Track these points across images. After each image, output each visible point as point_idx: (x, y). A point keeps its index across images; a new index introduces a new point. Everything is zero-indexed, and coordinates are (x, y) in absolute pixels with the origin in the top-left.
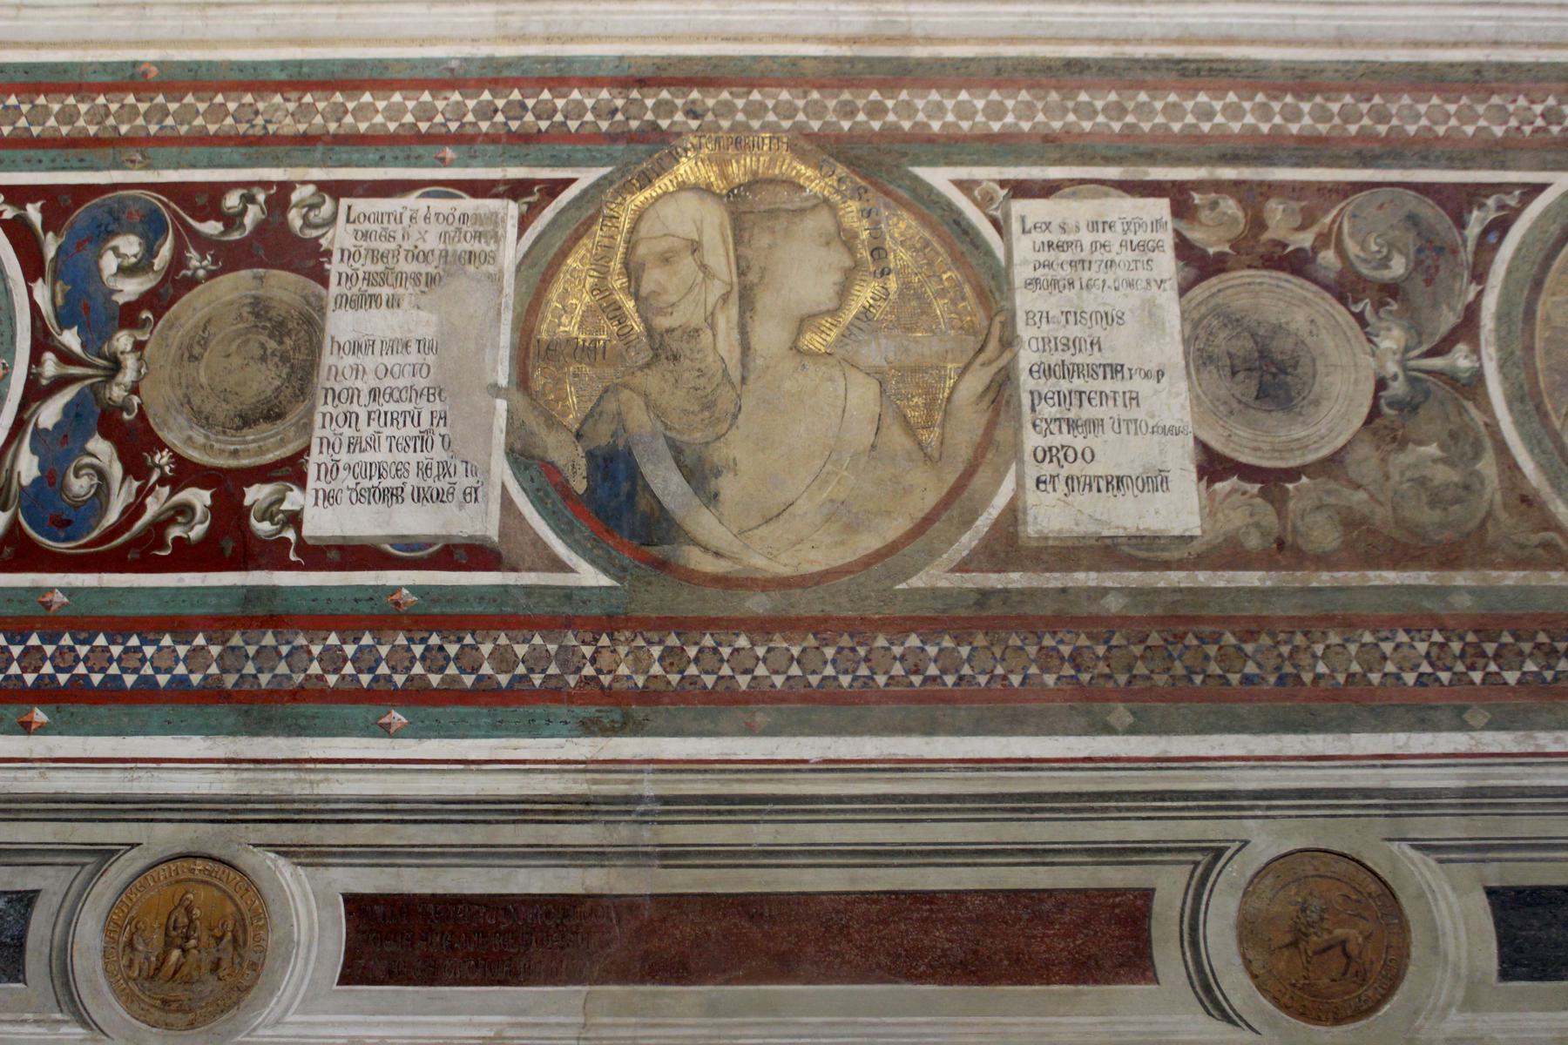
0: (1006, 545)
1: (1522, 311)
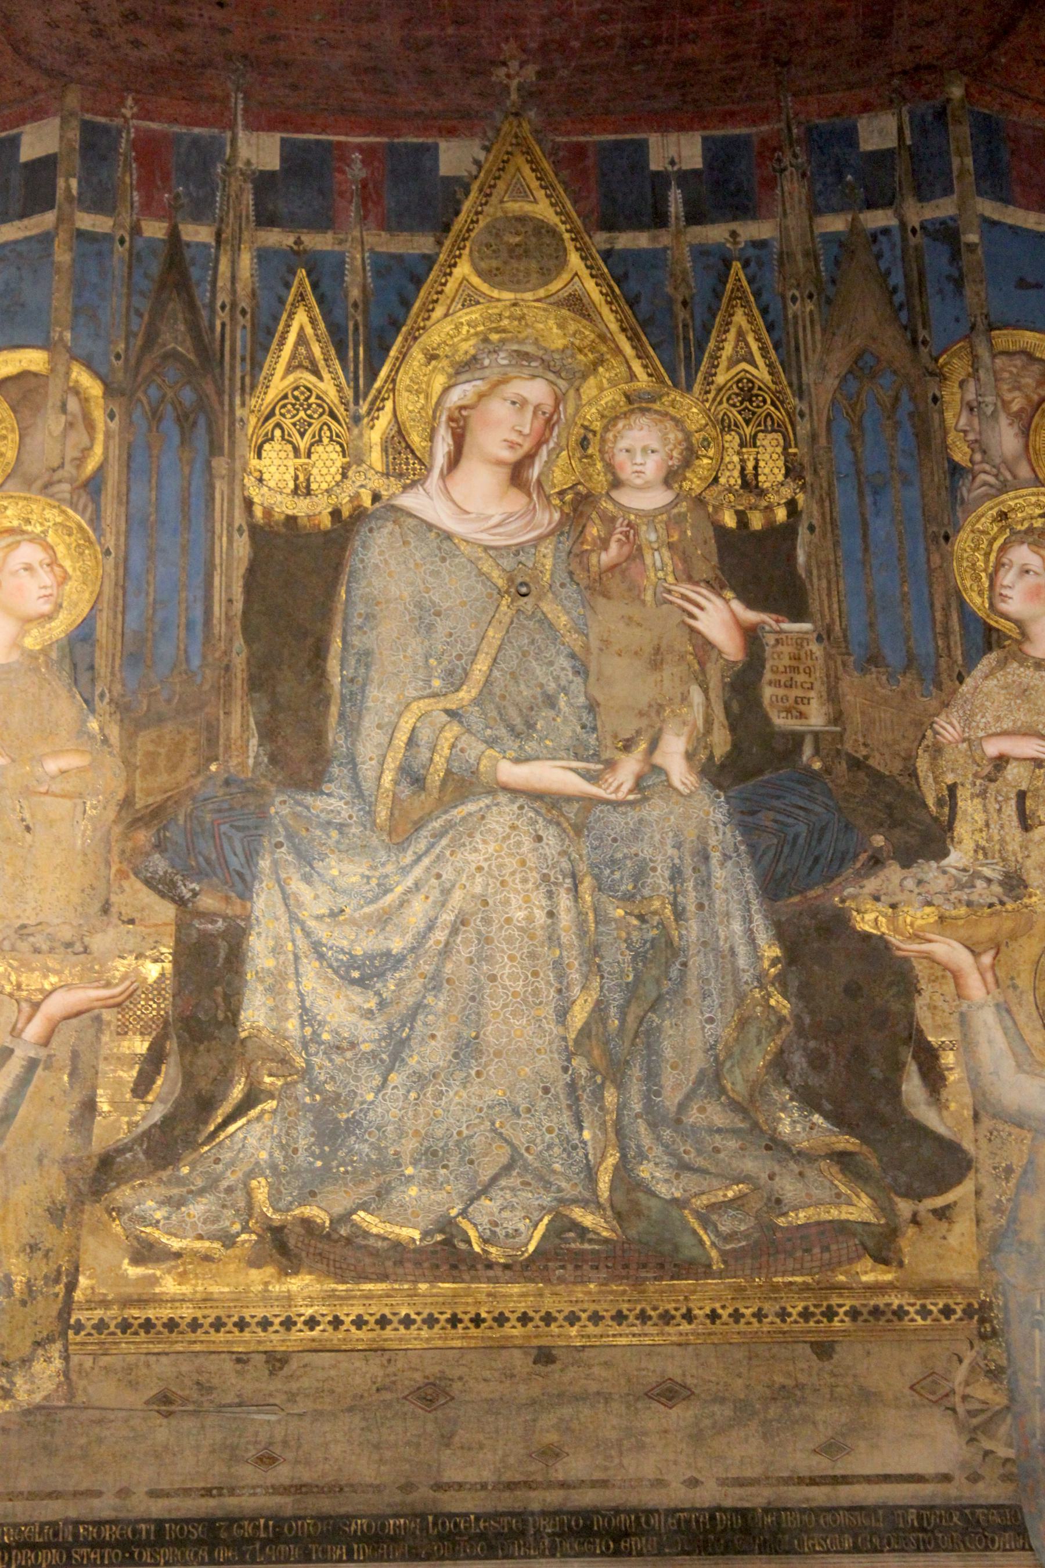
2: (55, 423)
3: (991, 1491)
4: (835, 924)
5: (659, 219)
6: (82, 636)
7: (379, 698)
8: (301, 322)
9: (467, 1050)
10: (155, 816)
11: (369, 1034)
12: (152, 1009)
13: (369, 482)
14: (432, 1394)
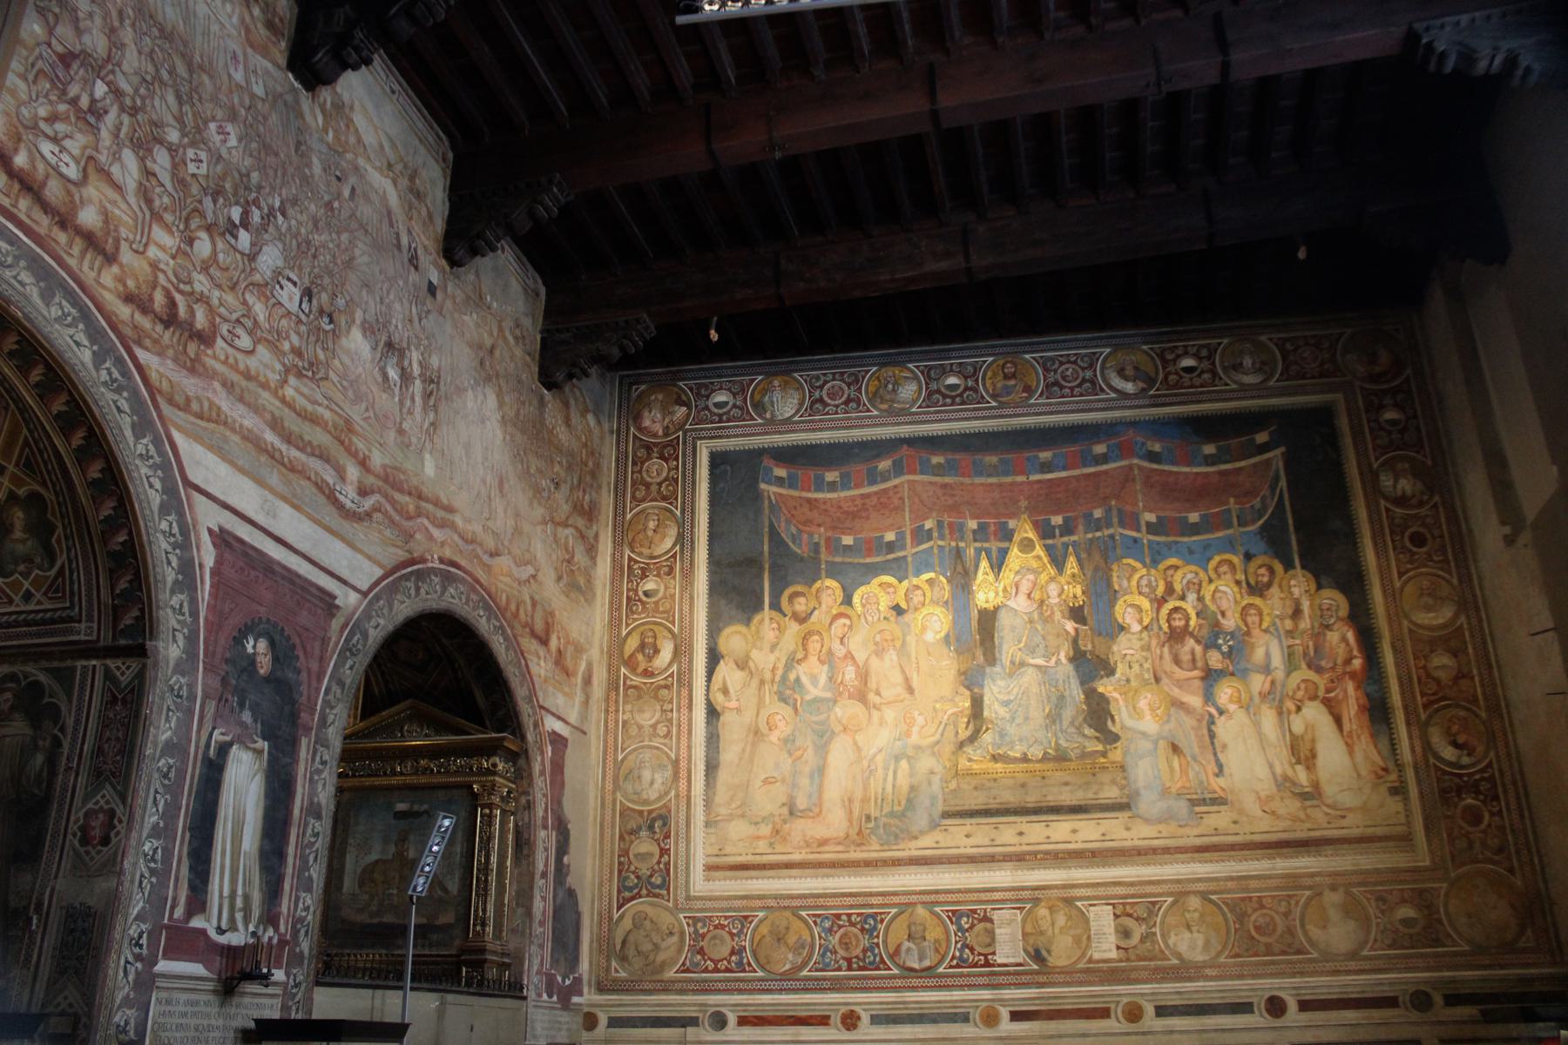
0: (1090, 961)
1: (1162, 922)
2: (936, 589)
3: (1124, 800)
4: (1094, 690)
5: (1054, 537)
6: (947, 636)
7: (1005, 647)
8: (984, 564)
9: (1026, 718)
10: (964, 673)
11: (1008, 716)
12: (968, 712)
13: (1000, 600)
14: (1023, 785)
